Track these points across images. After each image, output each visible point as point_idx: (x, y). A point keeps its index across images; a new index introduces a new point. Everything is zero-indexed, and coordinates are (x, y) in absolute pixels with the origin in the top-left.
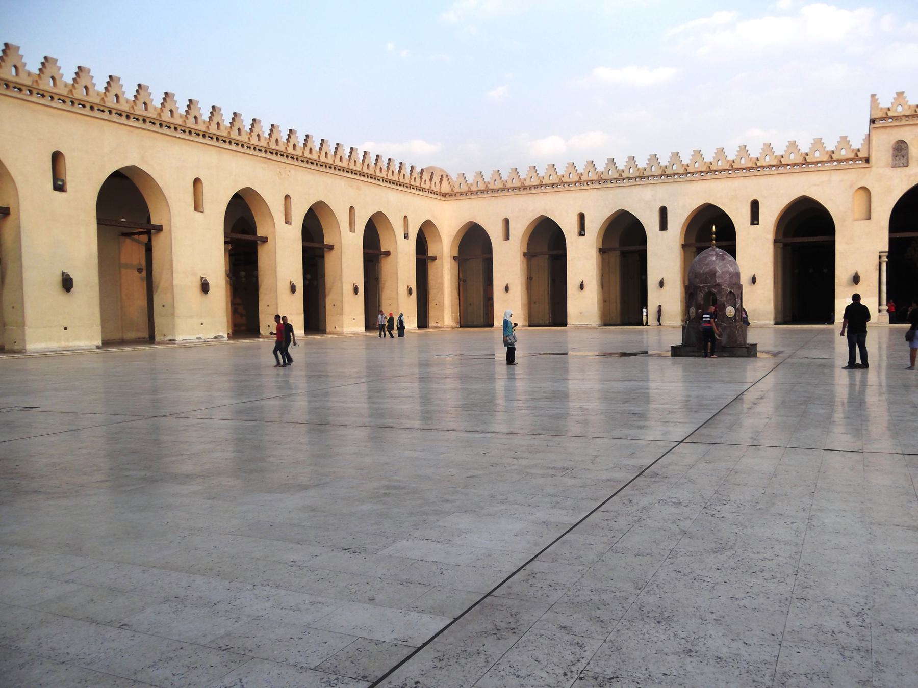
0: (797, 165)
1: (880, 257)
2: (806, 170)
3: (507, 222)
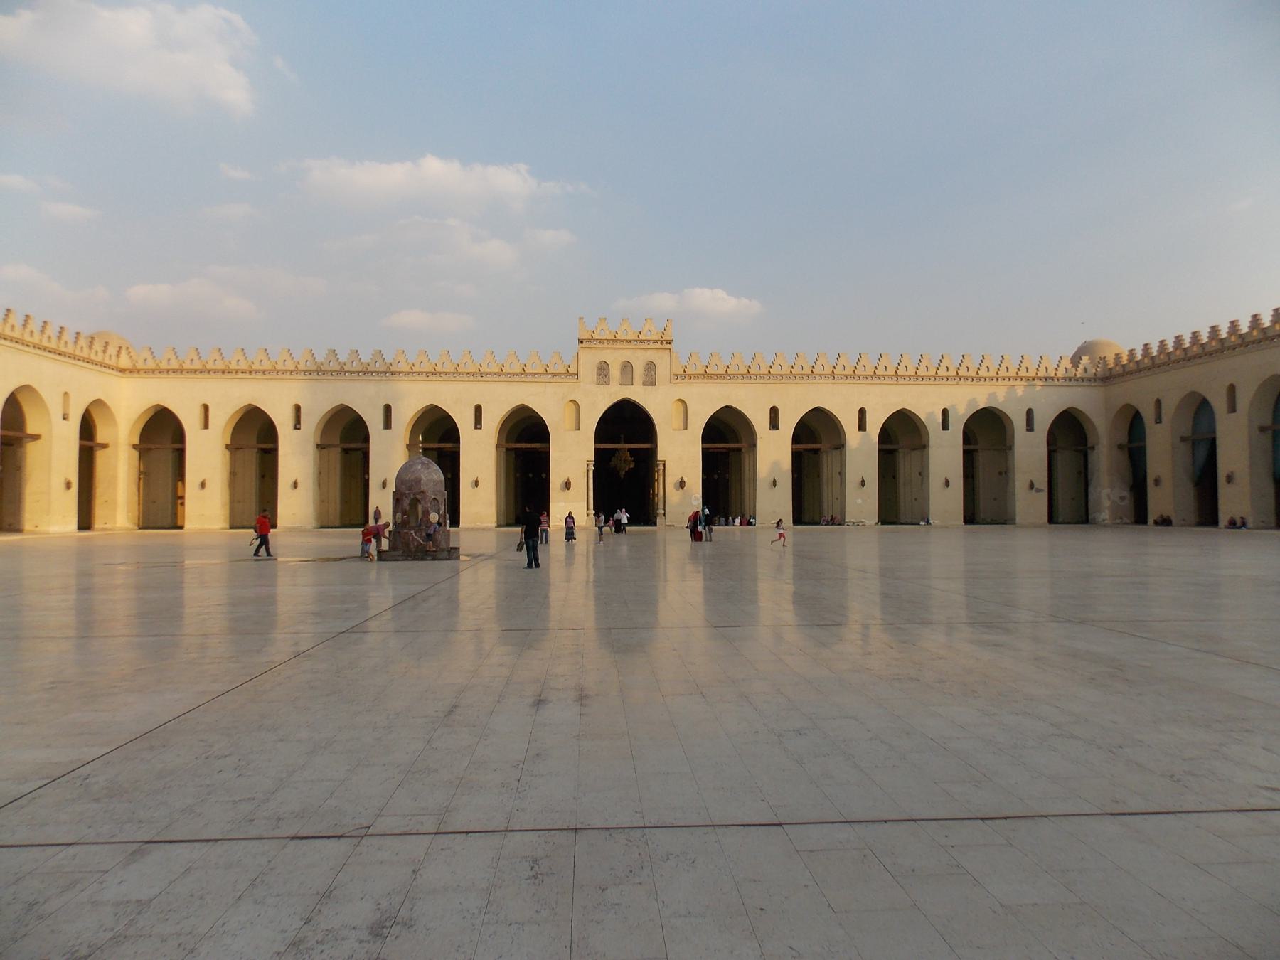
0: (517, 374)
2: (524, 380)
3: (206, 408)
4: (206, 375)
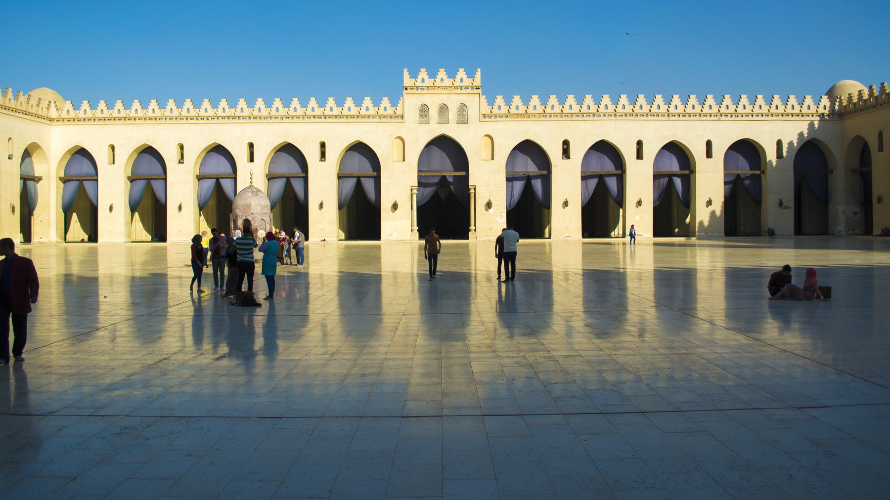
1: (412, 190)
4: (112, 122)
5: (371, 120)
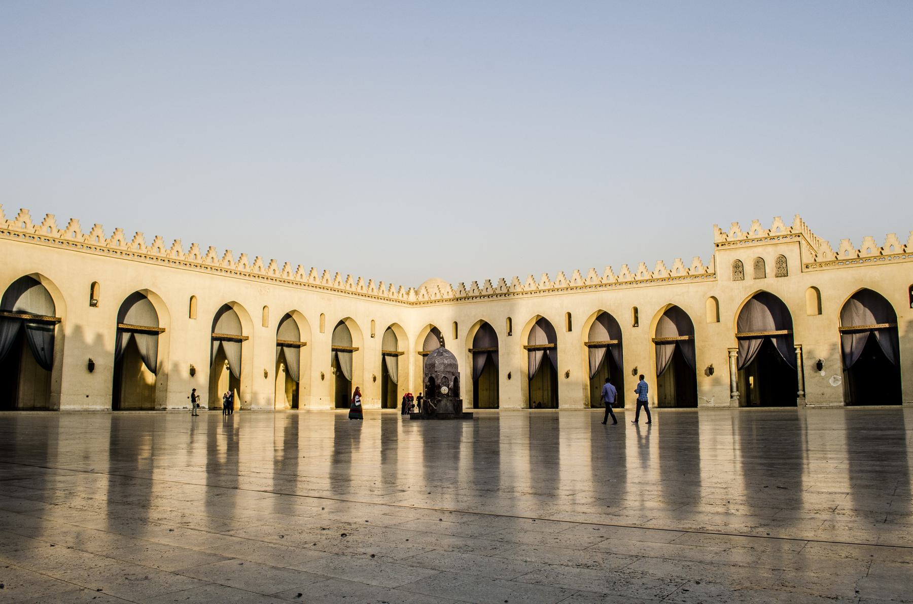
1: (729, 352)
5: (683, 281)
